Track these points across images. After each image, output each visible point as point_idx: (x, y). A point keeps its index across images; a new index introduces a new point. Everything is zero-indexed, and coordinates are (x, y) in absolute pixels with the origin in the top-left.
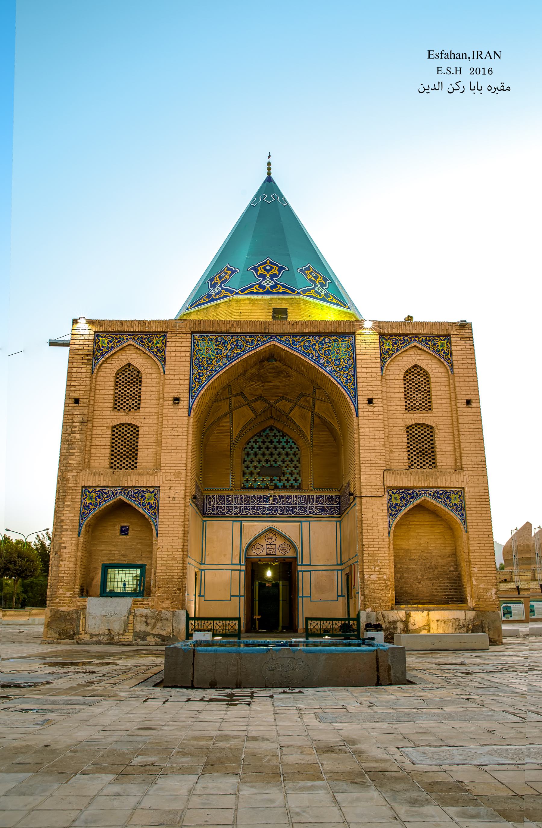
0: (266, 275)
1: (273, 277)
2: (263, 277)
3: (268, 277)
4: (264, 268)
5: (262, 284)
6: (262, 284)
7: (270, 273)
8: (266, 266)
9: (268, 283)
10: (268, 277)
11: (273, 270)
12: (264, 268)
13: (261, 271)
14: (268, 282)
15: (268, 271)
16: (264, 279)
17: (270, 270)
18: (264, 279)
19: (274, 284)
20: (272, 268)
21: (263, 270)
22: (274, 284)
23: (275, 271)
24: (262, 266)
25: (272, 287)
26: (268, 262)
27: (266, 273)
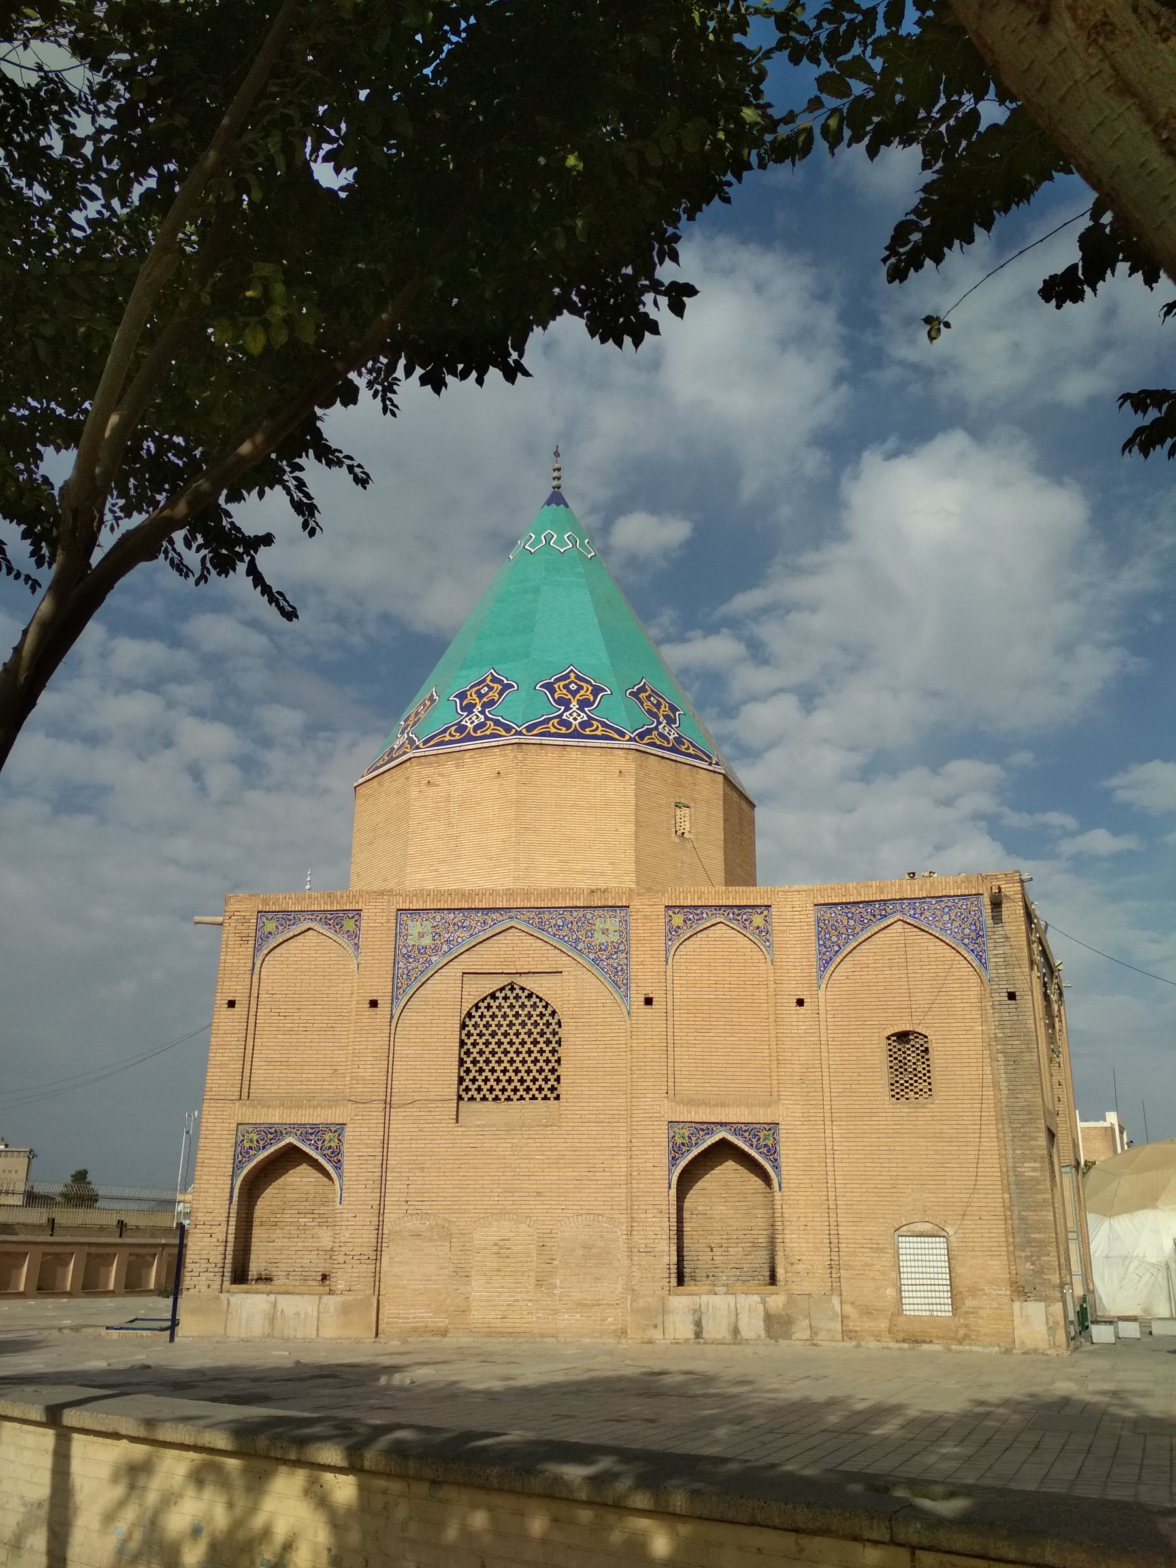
0: (569, 701)
1: (584, 704)
2: (566, 703)
3: (574, 705)
4: (564, 687)
5: (564, 717)
6: (564, 717)
7: (578, 697)
8: (570, 683)
9: (575, 717)
10: (574, 705)
11: (582, 692)
12: (564, 687)
13: (561, 692)
14: (575, 715)
15: (574, 693)
16: (567, 709)
17: (577, 691)
18: (567, 709)
19: (586, 718)
20: (581, 688)
21: (565, 691)
22: (586, 718)
23: (586, 693)
24: (562, 684)
25: (584, 725)
26: (572, 674)
27: (570, 696)
